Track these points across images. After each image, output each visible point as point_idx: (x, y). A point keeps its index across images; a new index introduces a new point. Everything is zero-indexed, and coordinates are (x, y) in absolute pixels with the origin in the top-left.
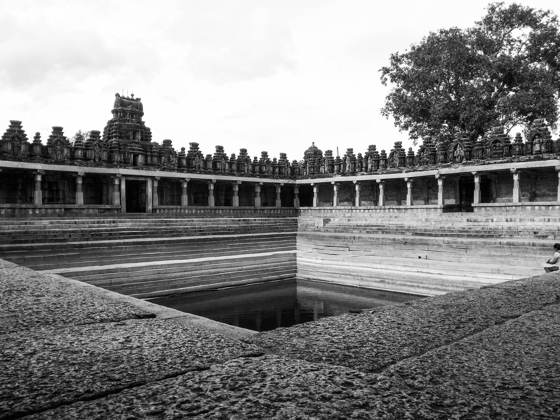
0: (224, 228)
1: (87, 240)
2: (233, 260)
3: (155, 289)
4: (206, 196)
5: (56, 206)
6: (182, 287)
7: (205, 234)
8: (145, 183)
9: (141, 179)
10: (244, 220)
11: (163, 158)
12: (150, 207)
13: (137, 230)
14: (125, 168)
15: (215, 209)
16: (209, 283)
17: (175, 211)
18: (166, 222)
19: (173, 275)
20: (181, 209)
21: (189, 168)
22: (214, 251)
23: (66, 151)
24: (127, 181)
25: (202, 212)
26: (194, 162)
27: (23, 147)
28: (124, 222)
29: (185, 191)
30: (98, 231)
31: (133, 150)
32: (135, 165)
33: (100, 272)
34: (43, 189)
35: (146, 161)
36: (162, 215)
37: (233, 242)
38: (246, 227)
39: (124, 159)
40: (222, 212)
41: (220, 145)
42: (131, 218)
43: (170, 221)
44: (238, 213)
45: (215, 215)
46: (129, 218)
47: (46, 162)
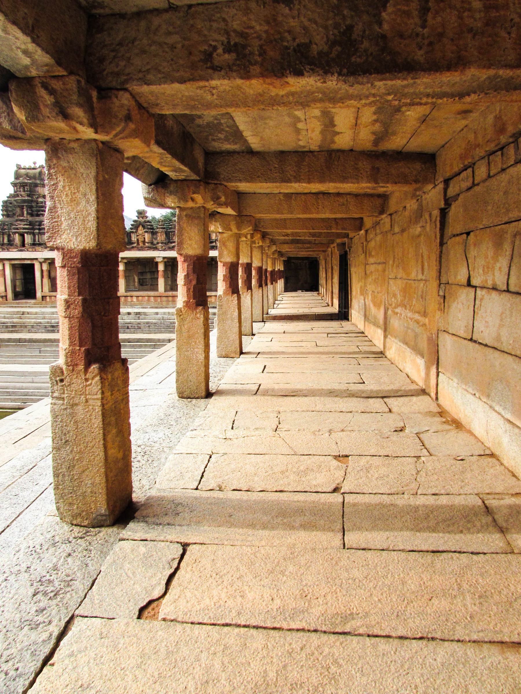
4: (156, 276)
7: (53, 331)
8: (33, 265)
12: (39, 294)
15: (125, 296)
18: (23, 313)
22: (8, 357)
24: (14, 267)
31: (17, 229)
35: (34, 240)
39: (9, 240)
40: (138, 300)
42: (12, 307)
43: (28, 313)
46: (10, 307)
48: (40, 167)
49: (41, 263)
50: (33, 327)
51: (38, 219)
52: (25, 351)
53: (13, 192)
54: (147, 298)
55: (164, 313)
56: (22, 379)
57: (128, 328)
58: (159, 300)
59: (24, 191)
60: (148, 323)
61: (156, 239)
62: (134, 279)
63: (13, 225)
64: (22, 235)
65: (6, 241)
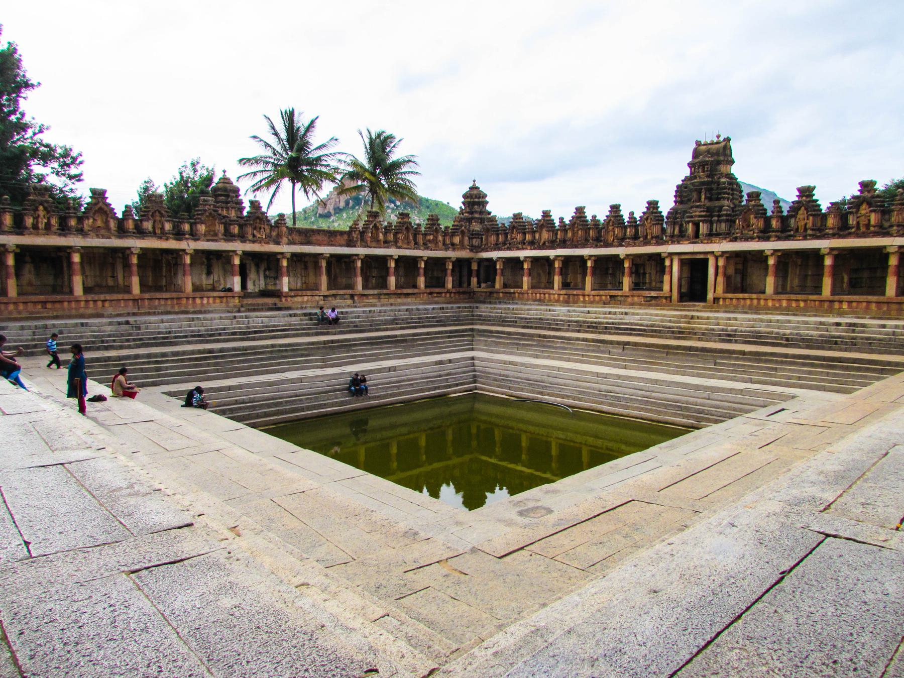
0: (784, 334)
1: (579, 331)
2: (656, 382)
3: (522, 390)
4: (879, 274)
5: (602, 292)
6: (548, 395)
7: (730, 341)
9: (699, 257)
10: (850, 325)
11: (737, 221)
12: (710, 296)
13: (641, 325)
14: (679, 243)
15: (832, 302)
16: (580, 399)
17: (748, 302)
18: (692, 317)
19: (556, 380)
20: (759, 299)
21: (782, 232)
22: (677, 366)
23: (616, 231)
24: (682, 263)
25: (802, 304)
26: (792, 221)
27: (580, 232)
28: (638, 314)
29: (771, 270)
30: (600, 323)
31: (692, 217)
32: (696, 237)
33: (505, 363)
34: (631, 273)
35: (711, 230)
36: (726, 306)
37: (729, 358)
38: (839, 337)
39: (681, 231)
41: (866, 178)
42: (677, 310)
43: (698, 318)
44: (887, 310)
45: (830, 311)
47: (597, 247)
48: (724, 140)
49: (717, 258)
50: (703, 334)
51: (717, 203)
52: (697, 361)
53: (688, 174)
54: (864, 304)
55: (896, 327)
56: (696, 393)
57: (836, 343)
58: (885, 309)
59: (703, 171)
60: (867, 338)
61: (889, 220)
62: (843, 278)
63: (685, 212)
64: (697, 225)
65: (677, 231)
